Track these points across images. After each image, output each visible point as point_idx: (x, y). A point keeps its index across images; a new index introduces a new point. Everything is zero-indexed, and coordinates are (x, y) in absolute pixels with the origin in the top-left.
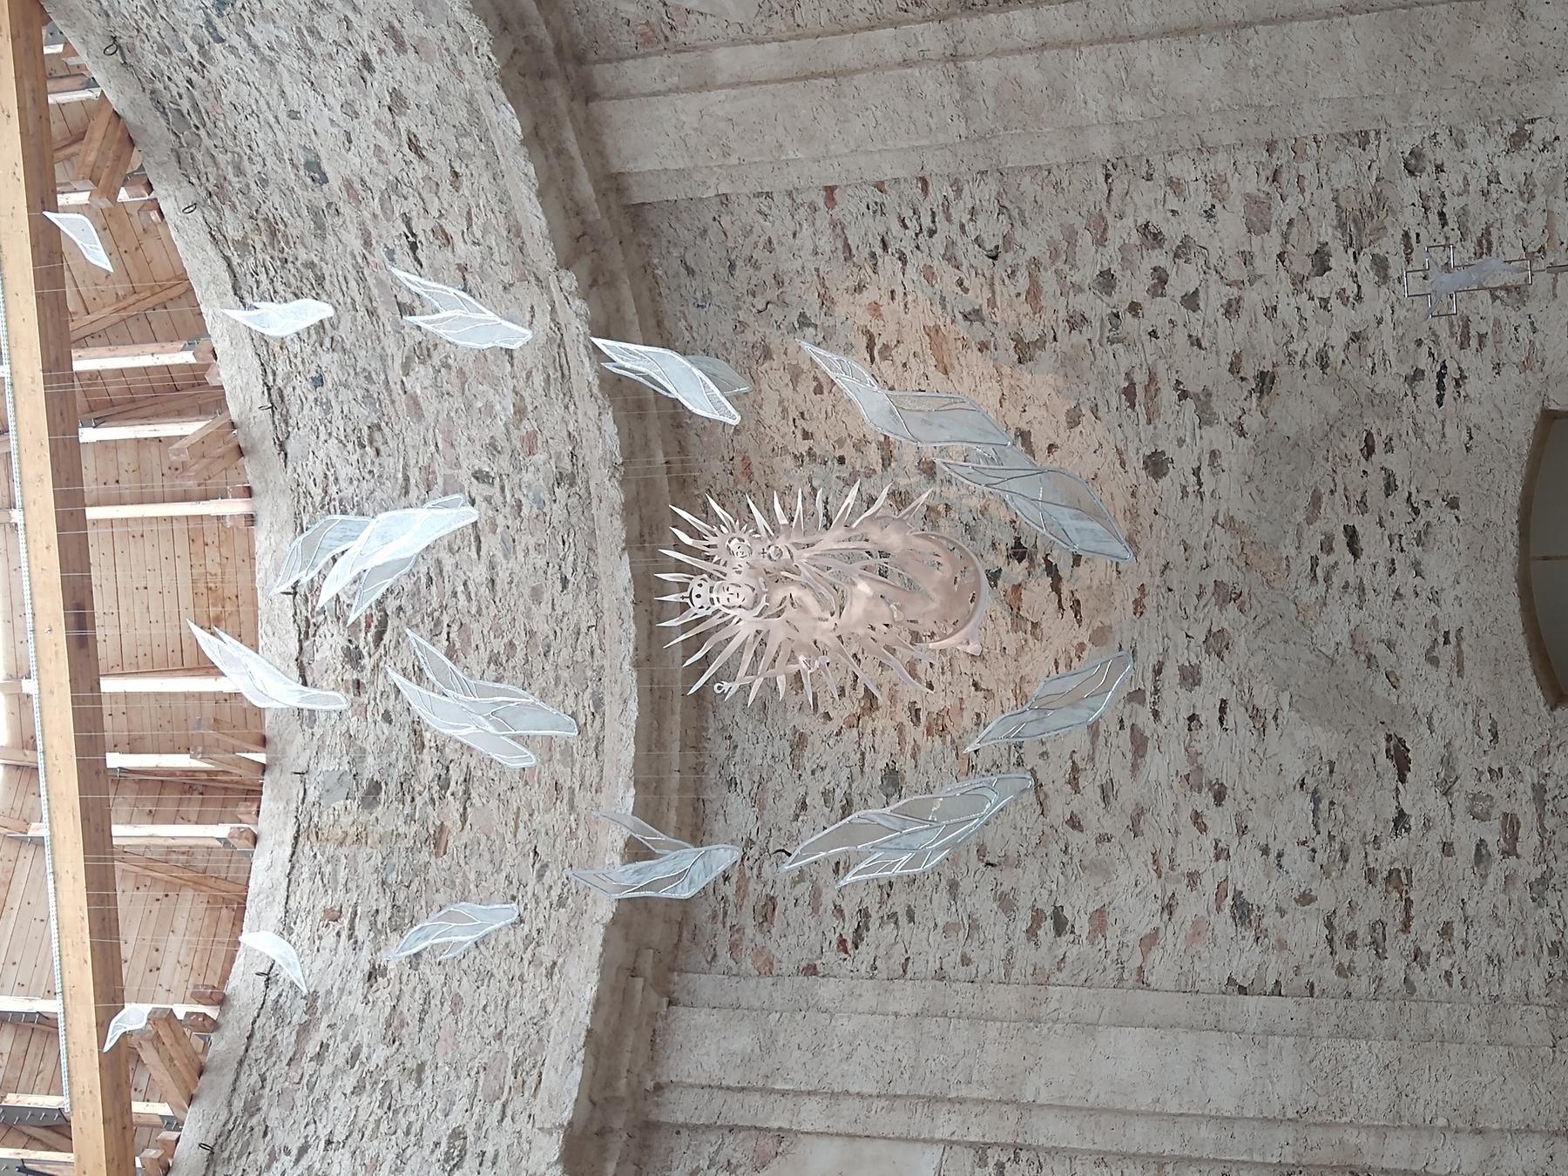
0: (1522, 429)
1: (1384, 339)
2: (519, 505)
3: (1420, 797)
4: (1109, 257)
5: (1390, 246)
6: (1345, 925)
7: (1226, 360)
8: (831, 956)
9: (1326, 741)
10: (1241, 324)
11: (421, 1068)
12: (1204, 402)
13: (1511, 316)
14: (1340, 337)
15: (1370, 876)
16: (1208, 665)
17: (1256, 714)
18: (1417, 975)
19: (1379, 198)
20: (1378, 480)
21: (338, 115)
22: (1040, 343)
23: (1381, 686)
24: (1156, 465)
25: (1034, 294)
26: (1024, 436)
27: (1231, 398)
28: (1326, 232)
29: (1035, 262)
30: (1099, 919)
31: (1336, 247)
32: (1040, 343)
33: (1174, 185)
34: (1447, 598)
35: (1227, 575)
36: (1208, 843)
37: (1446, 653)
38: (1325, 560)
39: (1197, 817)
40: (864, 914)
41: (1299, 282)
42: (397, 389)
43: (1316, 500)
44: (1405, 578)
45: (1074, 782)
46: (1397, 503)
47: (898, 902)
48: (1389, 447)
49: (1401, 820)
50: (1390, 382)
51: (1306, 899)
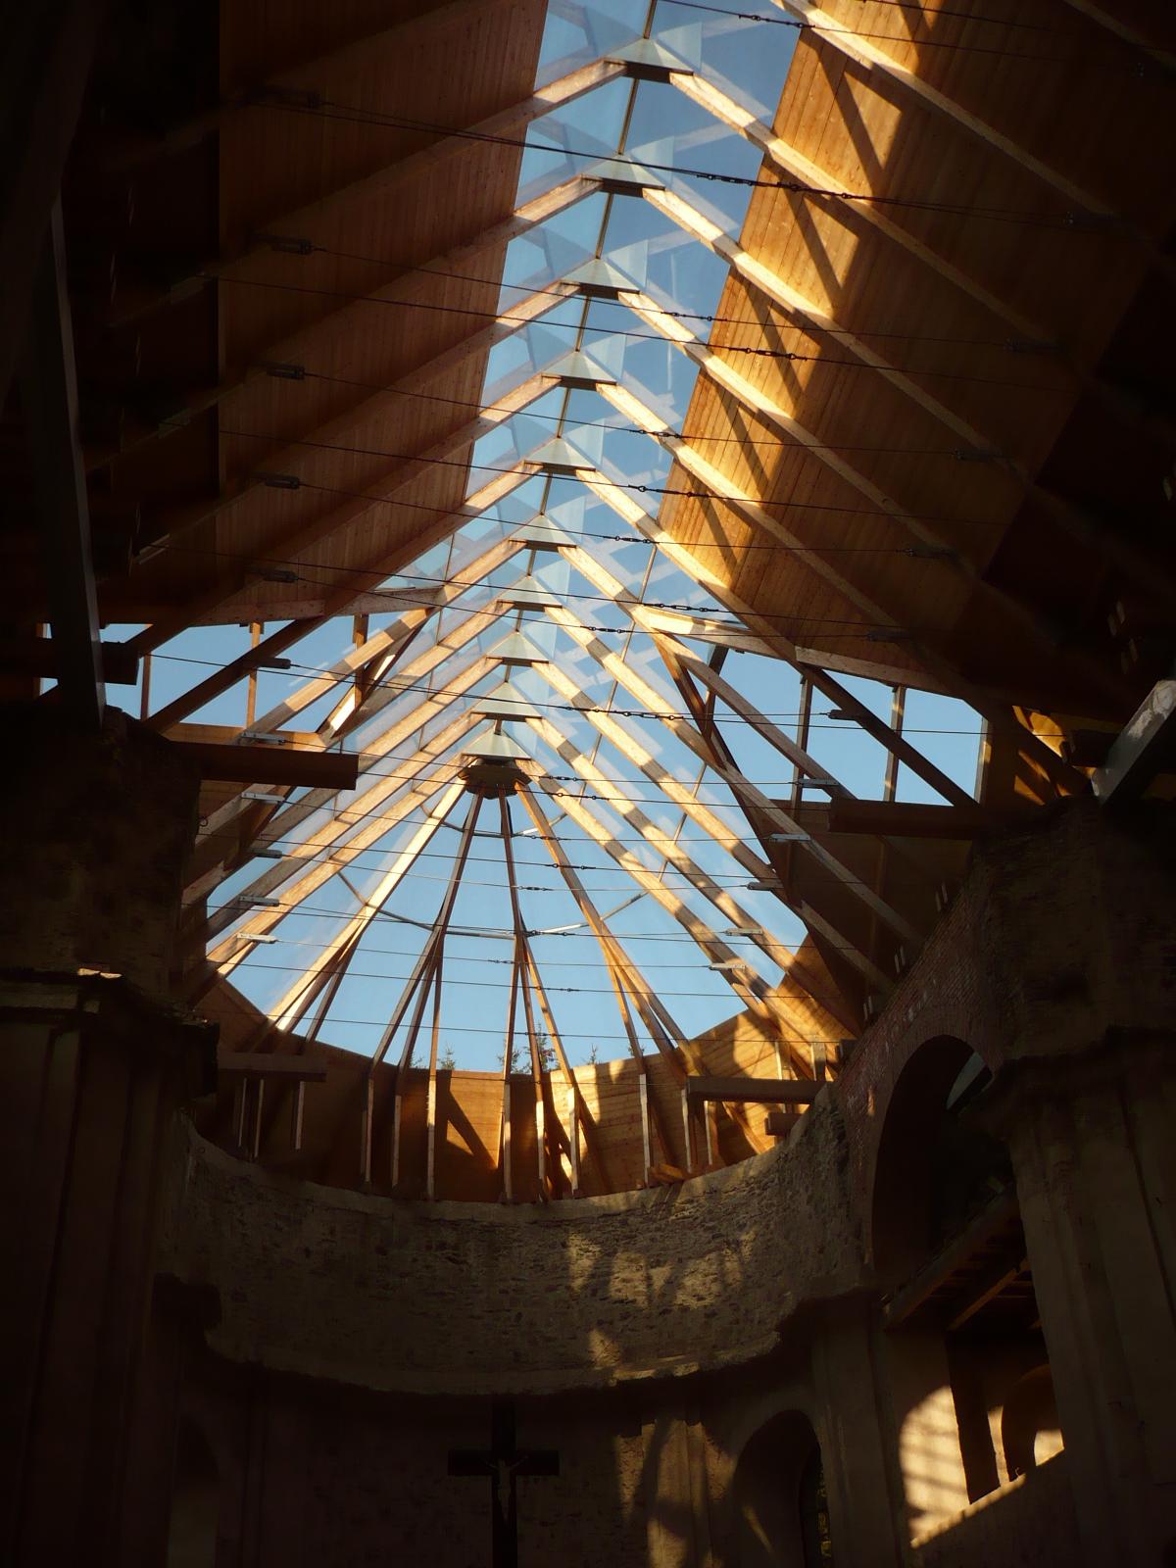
2: (505, 1333)
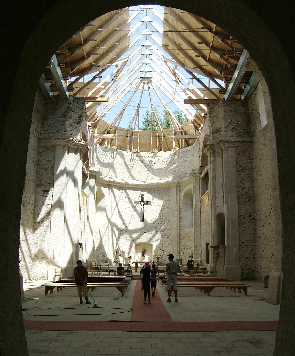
7: (157, 225)
10: (159, 226)
11: (112, 166)
16: (138, 223)
19: (166, 235)
26: (153, 212)
28: (164, 232)
31: (164, 233)
33: (168, 223)
42: (159, 166)
46: (148, 235)
47: (123, 202)
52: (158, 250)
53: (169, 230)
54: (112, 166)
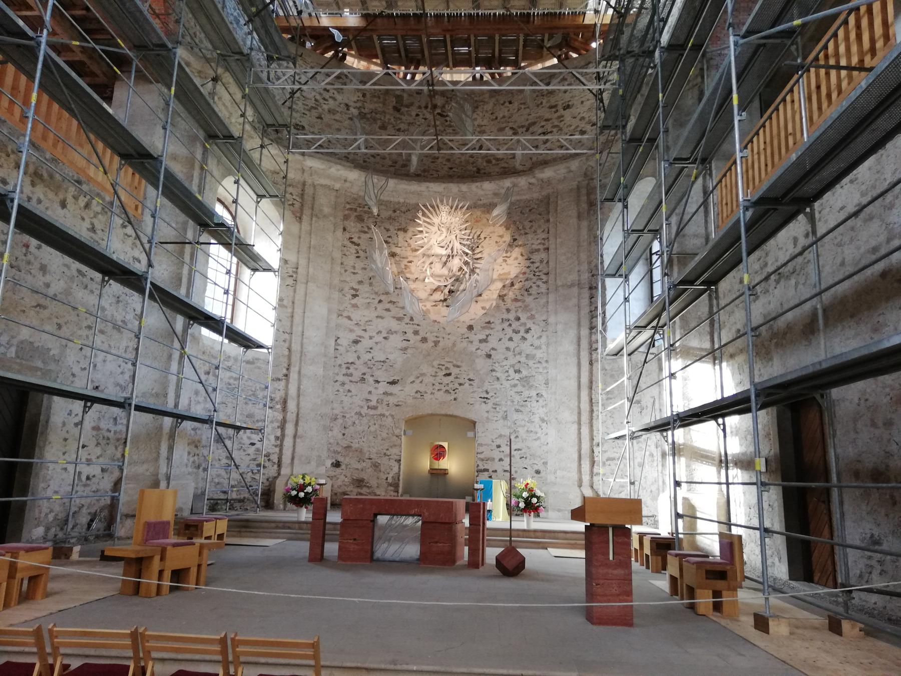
0: (472, 416)
1: (497, 385)
3: (383, 387)
4: (523, 320)
5: (519, 388)
6: (352, 367)
8: (348, 235)
9: (398, 366)
12: (484, 341)
13: (500, 415)
14: (498, 375)
15: (364, 374)
16: (419, 338)
17: (406, 349)
18: (338, 384)
20: (461, 381)
21: (581, 115)
22: (503, 300)
23: (411, 379)
24: (470, 328)
25: (516, 300)
26: (480, 295)
27: (485, 348)
28: (525, 373)
29: (524, 301)
30: (355, 306)
31: (521, 376)
32: (503, 300)
34: (432, 396)
35: (441, 344)
36: (374, 334)
37: (418, 395)
38: (443, 368)
39: (380, 332)
40: (358, 245)
41: (513, 366)
43: (458, 367)
44: (437, 387)
45: (391, 302)
46: (457, 386)
48: (470, 385)
49: (377, 382)
50: (487, 386)
51: (359, 358)
52: (499, 446)
53: (545, 365)
54: (321, 118)
